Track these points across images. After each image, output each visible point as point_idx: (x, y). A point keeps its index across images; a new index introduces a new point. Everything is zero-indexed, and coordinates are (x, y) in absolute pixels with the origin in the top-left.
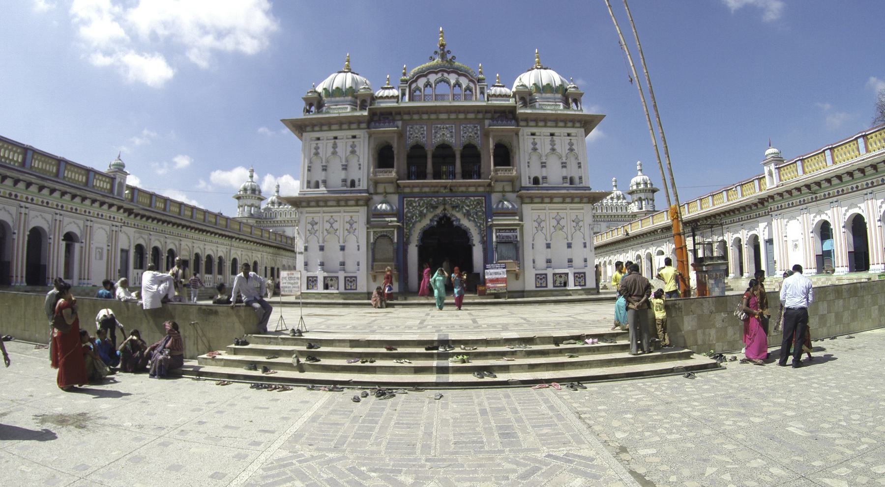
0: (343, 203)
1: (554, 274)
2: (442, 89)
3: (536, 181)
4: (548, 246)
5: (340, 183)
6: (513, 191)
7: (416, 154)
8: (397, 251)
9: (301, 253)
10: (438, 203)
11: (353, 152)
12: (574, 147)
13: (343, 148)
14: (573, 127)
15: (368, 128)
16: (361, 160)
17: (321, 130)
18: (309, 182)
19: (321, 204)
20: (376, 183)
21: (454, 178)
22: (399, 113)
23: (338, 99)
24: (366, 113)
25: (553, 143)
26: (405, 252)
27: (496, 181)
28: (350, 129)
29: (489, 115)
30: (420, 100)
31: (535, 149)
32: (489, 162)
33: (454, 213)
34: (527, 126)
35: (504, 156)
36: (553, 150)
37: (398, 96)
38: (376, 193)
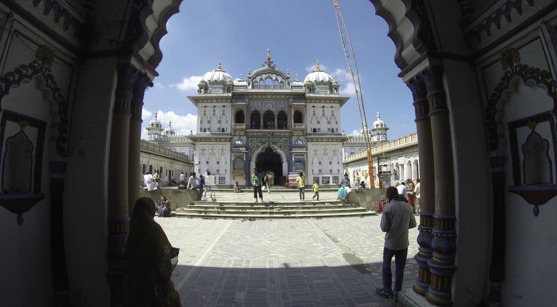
0: (218, 140)
1: (323, 177)
2: (269, 82)
3: (315, 130)
4: (320, 163)
5: (217, 130)
6: (303, 136)
7: (255, 115)
8: (245, 164)
10: (266, 141)
11: (223, 114)
13: (219, 112)
15: (231, 102)
16: (228, 118)
17: (207, 102)
18: (201, 129)
19: (207, 140)
20: (235, 130)
21: (274, 128)
22: (247, 95)
23: (215, 86)
24: (230, 95)
25: (323, 111)
26: (249, 165)
27: (295, 130)
28: (222, 102)
29: (292, 97)
30: (257, 88)
31: (314, 114)
32: (291, 120)
33: (273, 146)
34: (311, 102)
35: (299, 118)
36: (324, 115)
38: (235, 135)
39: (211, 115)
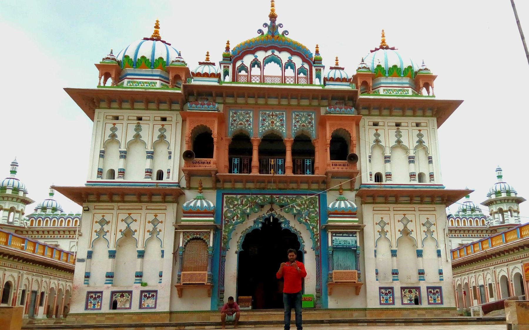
3: (378, 177)
6: (351, 190)
9: (82, 260)
11: (162, 137)
12: (423, 139)
14: (424, 116)
16: (172, 149)
17: (121, 108)
20: (190, 175)
25: (398, 134)
28: (158, 109)
31: (377, 141)
34: (369, 115)
36: (399, 142)
37: (219, 75)
38: (189, 188)
39: (130, 138)
